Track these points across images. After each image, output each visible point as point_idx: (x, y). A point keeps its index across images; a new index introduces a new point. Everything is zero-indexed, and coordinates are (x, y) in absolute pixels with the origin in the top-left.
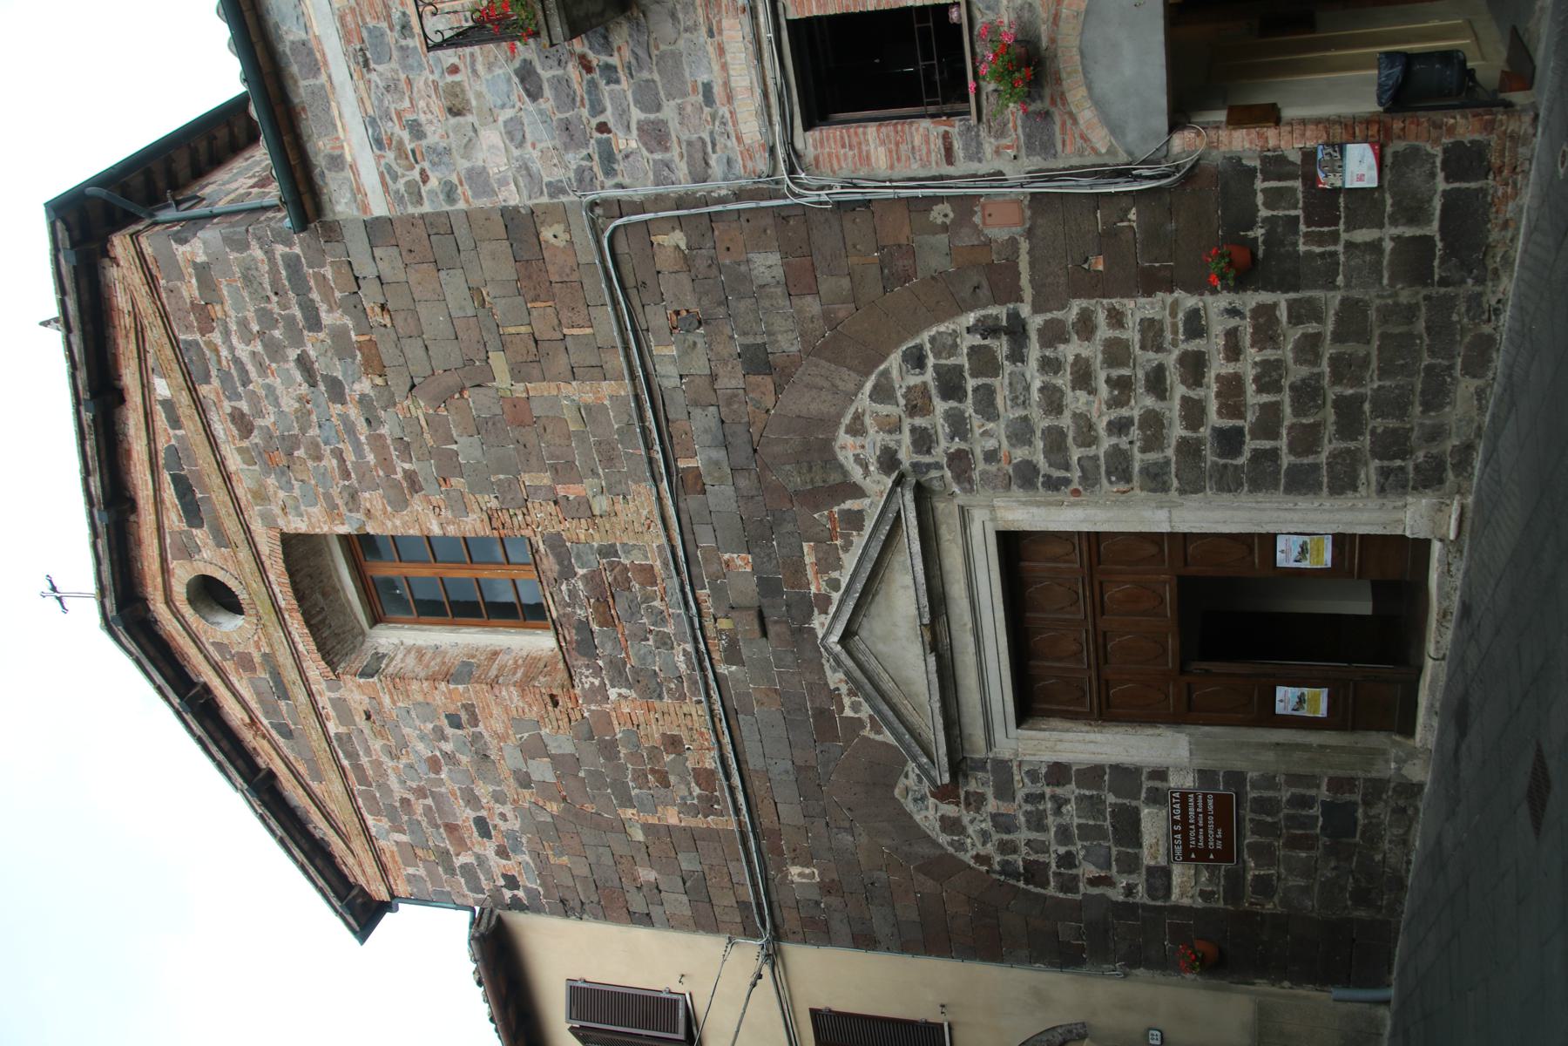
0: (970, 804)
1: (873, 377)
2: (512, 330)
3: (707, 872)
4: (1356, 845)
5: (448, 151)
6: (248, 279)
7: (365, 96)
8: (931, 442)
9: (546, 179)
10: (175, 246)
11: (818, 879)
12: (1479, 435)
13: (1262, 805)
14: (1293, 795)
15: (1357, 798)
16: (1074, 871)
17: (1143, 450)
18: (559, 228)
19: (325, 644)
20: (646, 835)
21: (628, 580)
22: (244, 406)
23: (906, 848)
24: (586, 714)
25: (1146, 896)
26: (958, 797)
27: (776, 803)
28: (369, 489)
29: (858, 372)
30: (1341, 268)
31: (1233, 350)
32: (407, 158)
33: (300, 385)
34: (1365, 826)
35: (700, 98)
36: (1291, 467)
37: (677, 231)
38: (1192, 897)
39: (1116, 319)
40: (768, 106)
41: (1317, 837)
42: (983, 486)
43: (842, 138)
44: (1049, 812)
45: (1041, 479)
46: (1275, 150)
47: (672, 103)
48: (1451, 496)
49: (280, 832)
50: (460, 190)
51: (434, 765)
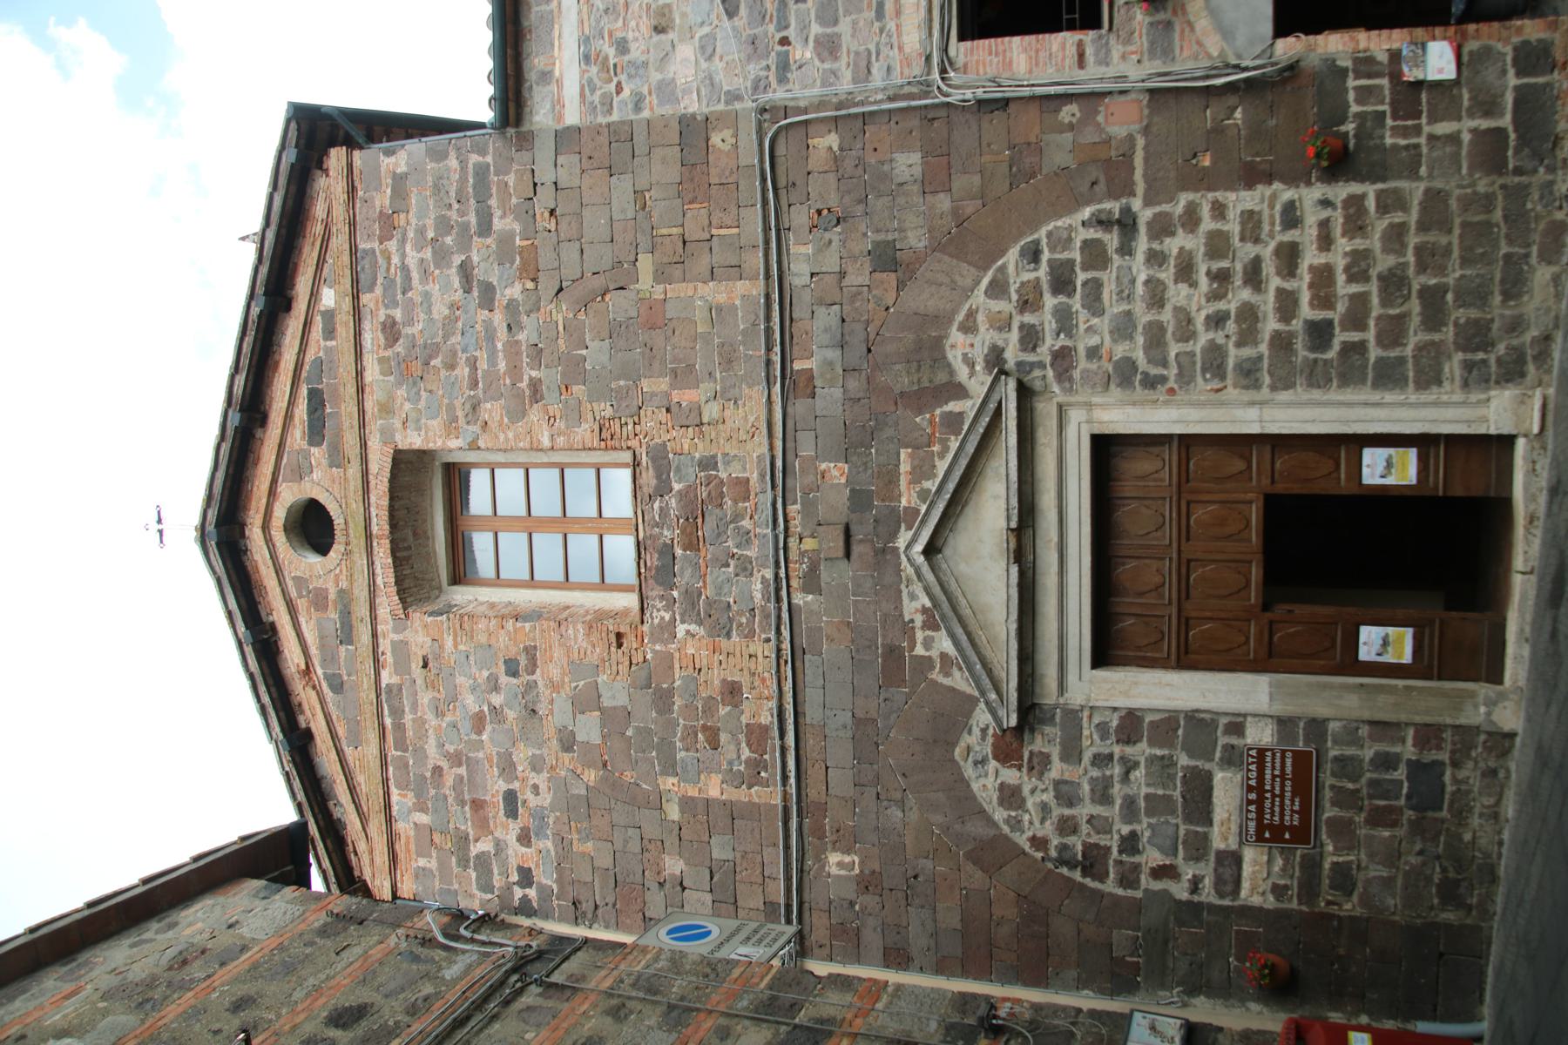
0: (1033, 768)
1: (990, 274)
2: (665, 231)
3: (738, 861)
4: (1443, 821)
5: (645, 64)
6: (437, 188)
7: (586, 17)
8: (1038, 339)
9: (726, 88)
10: (382, 157)
11: (857, 871)
12: (1556, 326)
13: (1346, 767)
14: (1377, 754)
15: (1444, 756)
16: (1136, 859)
17: (1239, 345)
18: (727, 133)
19: (403, 580)
20: (682, 812)
21: (722, 495)
22: (398, 314)
24: (649, 657)
25: (1213, 892)
26: (1021, 758)
27: (827, 768)
28: (493, 399)
29: (978, 267)
30: (1424, 159)
31: (1325, 242)
32: (608, 71)
34: (1453, 794)
35: (873, 13)
36: (1379, 360)
37: (833, 134)
38: (1263, 894)
39: (1219, 210)
40: (931, 20)
41: (1400, 810)
42: (1082, 386)
43: (990, 46)
44: (1116, 779)
45: (1139, 377)
46: (1365, 51)
47: (848, 19)
48: (1533, 388)
49: (301, 796)
50: (647, 101)
51: (479, 722)
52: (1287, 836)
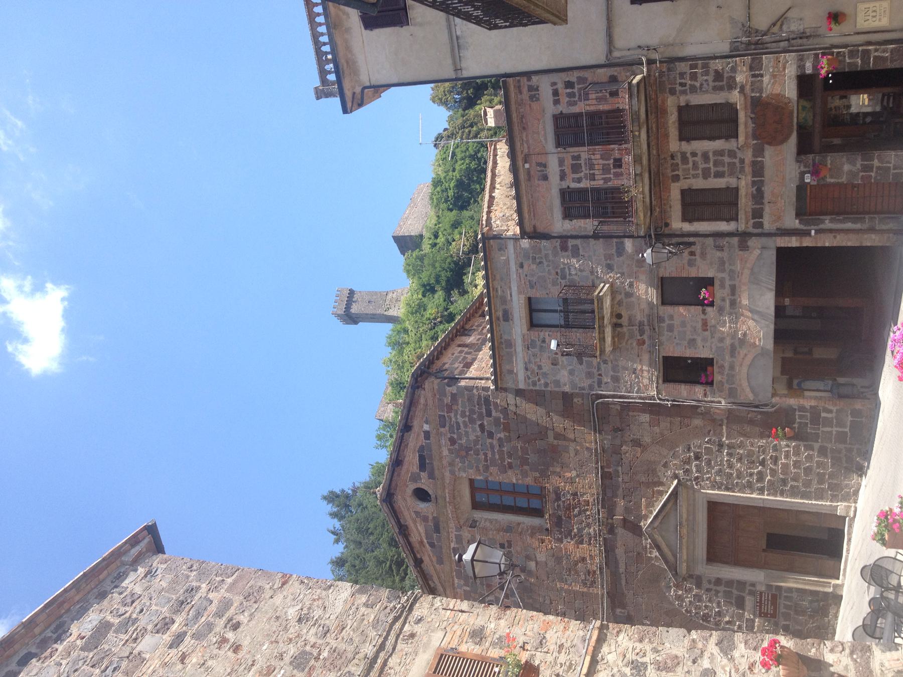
10: (446, 387)
18: (580, 399)
22: (455, 436)
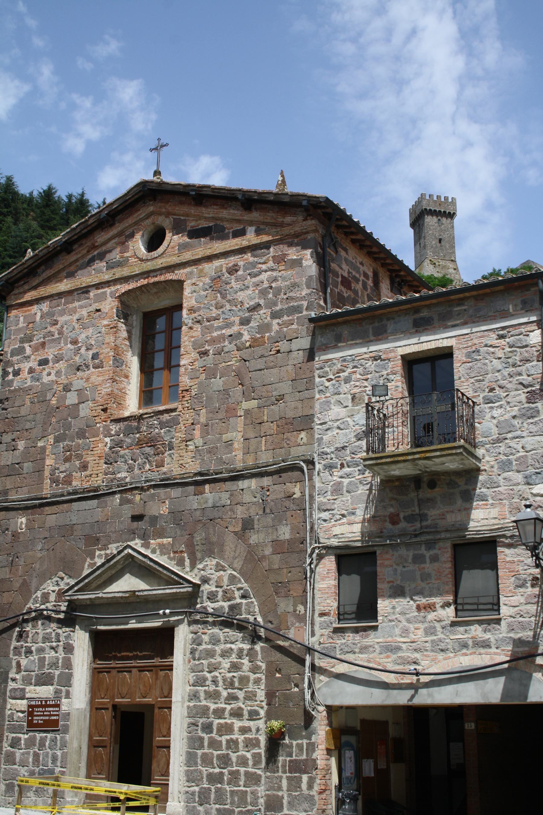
1: (238, 575)
3: (23, 476)
9: (324, 437)
11: (19, 531)
14: (57, 756)
17: (205, 691)
18: (305, 440)
20: (41, 447)
22: (240, 273)
23: (35, 575)
25: (12, 687)
26: (59, 602)
33: (248, 304)
36: (196, 753)
39: (257, 681)
50: (323, 396)
51: (75, 342)
52: (30, 718)
